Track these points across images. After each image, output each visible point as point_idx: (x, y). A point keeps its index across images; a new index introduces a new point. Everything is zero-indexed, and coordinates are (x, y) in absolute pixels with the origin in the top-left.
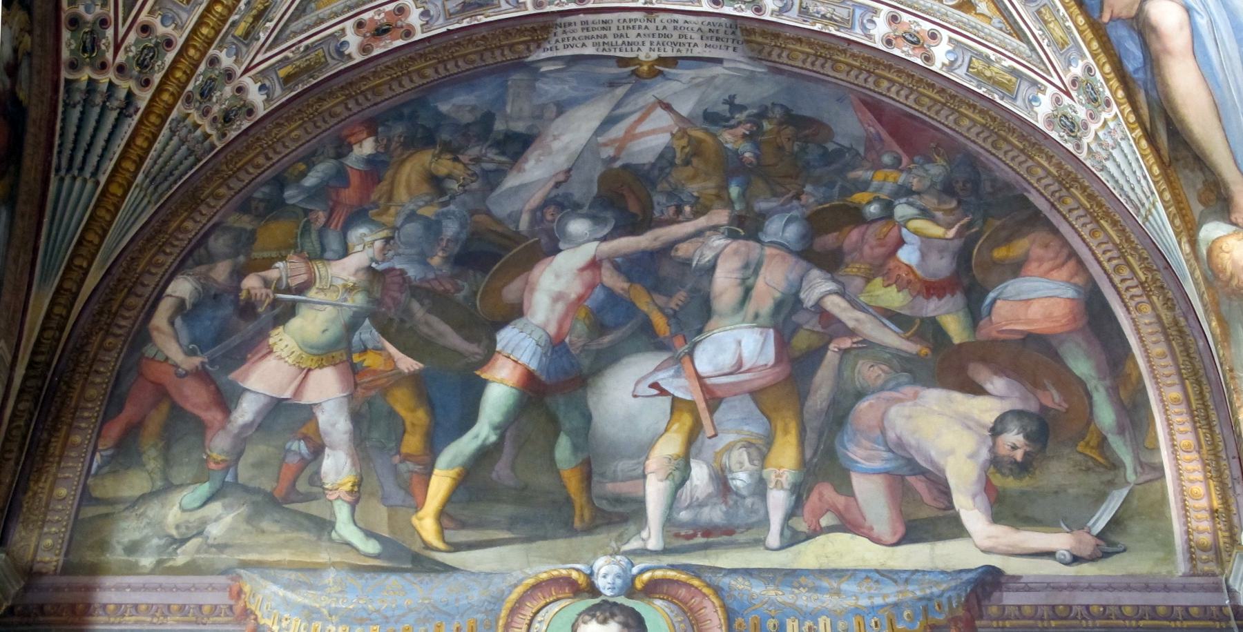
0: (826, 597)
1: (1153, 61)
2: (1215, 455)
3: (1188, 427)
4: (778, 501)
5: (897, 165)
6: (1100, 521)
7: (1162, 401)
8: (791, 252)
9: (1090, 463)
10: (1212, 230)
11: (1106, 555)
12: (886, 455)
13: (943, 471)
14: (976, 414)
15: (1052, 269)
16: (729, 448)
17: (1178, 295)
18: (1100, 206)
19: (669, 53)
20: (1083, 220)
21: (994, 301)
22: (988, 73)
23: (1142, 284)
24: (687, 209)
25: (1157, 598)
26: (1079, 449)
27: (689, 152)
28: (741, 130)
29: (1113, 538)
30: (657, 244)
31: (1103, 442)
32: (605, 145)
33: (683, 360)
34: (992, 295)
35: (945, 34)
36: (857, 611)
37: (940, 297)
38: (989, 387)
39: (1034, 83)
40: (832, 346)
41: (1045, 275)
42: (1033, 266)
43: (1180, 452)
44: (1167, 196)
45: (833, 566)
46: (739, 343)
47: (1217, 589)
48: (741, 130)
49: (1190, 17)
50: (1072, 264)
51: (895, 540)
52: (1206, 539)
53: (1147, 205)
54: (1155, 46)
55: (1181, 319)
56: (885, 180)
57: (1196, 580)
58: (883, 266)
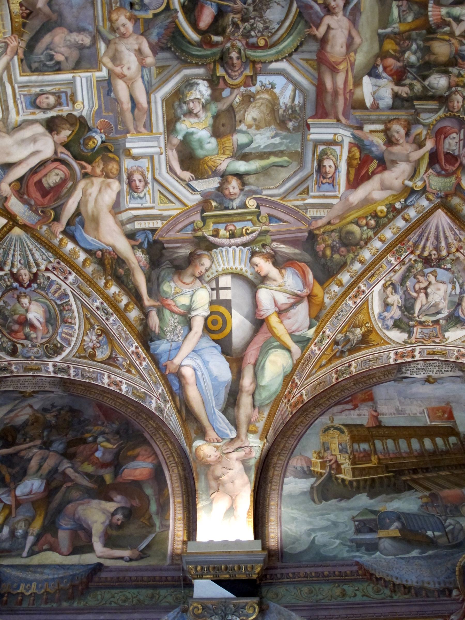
0: (38, 575)
1: (182, 387)
4: (31, 539)
5: (102, 425)
6: (143, 546)
7: (174, 503)
8: (59, 453)
10: (198, 443)
12: (72, 523)
13: (91, 529)
14: (108, 508)
16: (19, 521)
19: (37, 389)
21: (124, 469)
22: (138, 394)
24: (28, 439)
25: (157, 574)
27: (34, 421)
28: (53, 414)
30: (14, 452)
31: (150, 517)
32: (6, 419)
33: (11, 491)
34: (124, 467)
35: (124, 381)
36: (47, 580)
37: (106, 468)
38: (115, 499)
39: (150, 396)
40: (65, 486)
41: (144, 460)
42: (140, 457)
45: (43, 563)
46: (33, 485)
47: (179, 570)
48: (53, 414)
49: (195, 372)
50: (153, 456)
51: (67, 554)
52: (179, 551)
54: (184, 382)
56: (97, 429)
57: (172, 567)
58: (89, 459)
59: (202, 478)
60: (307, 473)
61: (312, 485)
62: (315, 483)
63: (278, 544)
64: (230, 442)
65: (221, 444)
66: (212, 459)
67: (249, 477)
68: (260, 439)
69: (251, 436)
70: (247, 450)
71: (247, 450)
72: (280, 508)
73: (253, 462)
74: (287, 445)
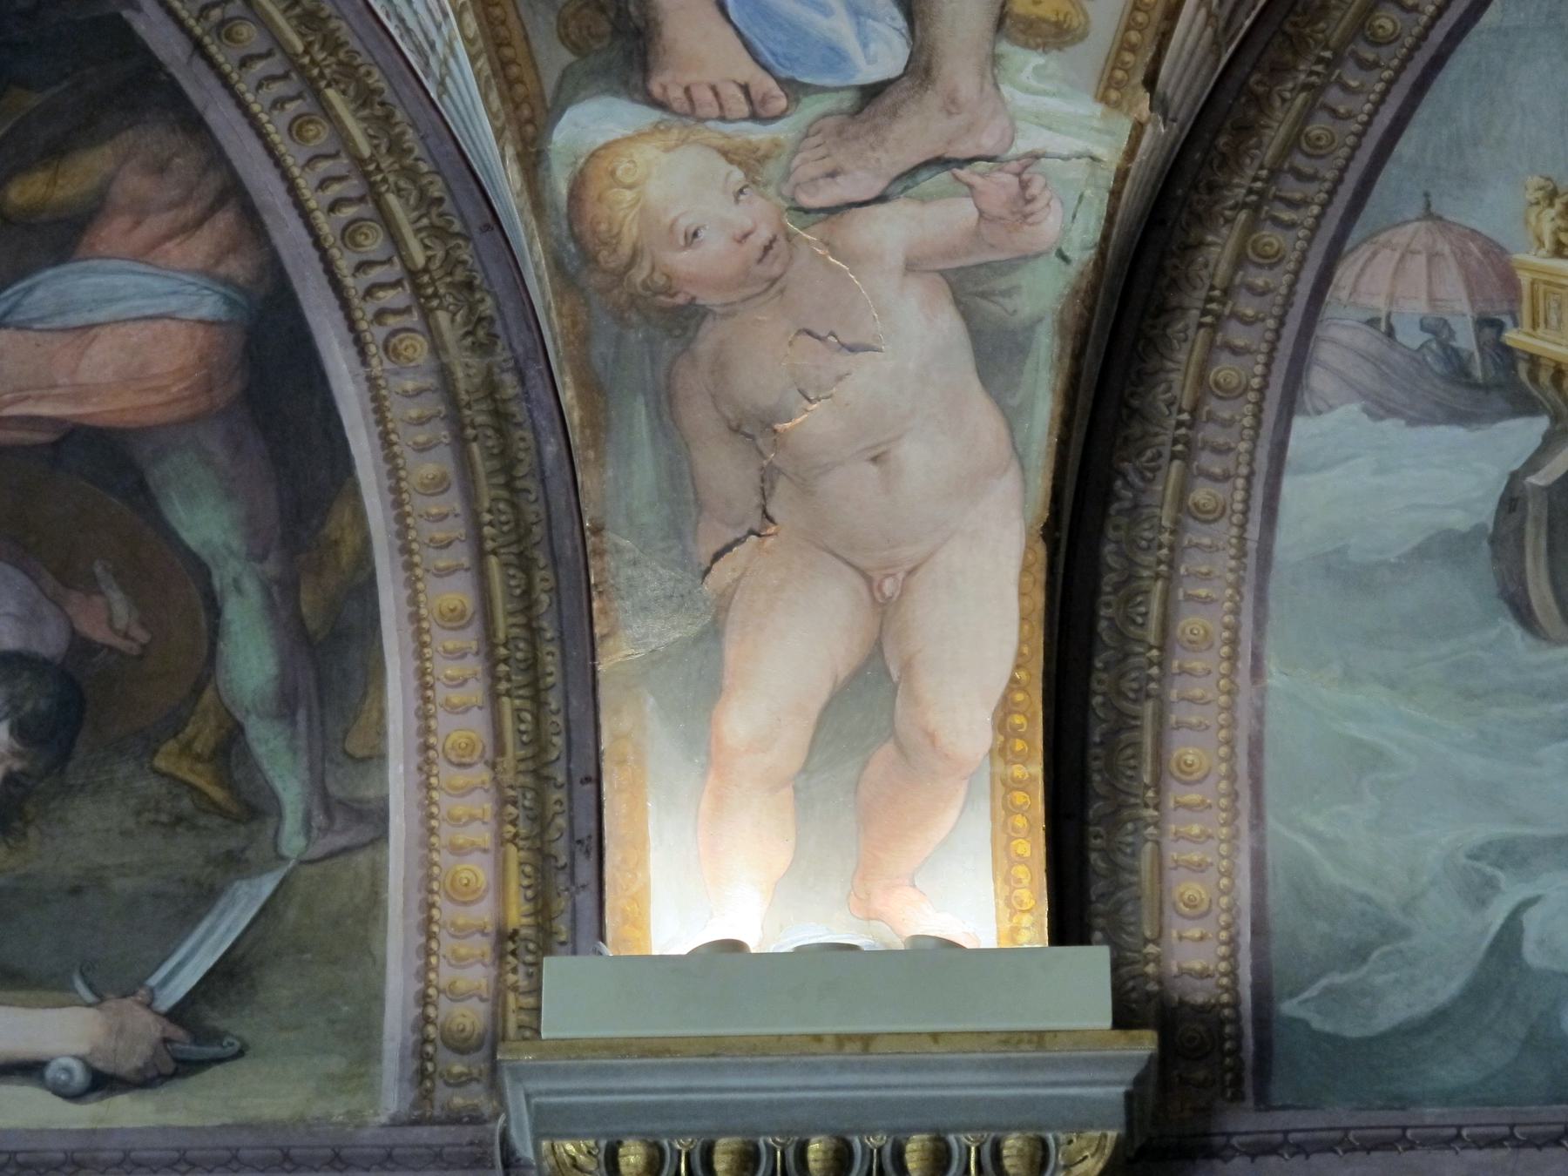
2: (535, 773)
3: (475, 692)
7: (416, 618)
9: (186, 804)
10: (591, 124)
11: (185, 1067)
15: (168, 237)
17: (510, 308)
18: (332, 44)
20: (278, 89)
23: (413, 274)
26: (161, 763)
29: (215, 1019)
41: (144, 254)
42: (112, 231)
43: (442, 767)
44: (472, 27)
50: (225, 220)
52: (469, 1016)
53: (439, 46)
55: (509, 379)
57: (424, 1134)
59: (639, 418)
60: (1485, 377)
61: (1515, 477)
62: (1532, 465)
63: (1232, 957)
64: (857, 112)
65: (783, 131)
66: (703, 263)
67: (1012, 418)
68: (1103, 99)
69: (1025, 63)
70: (998, 185)
71: (998, 185)
72: (1257, 671)
73: (1044, 295)
74: (1319, 127)
